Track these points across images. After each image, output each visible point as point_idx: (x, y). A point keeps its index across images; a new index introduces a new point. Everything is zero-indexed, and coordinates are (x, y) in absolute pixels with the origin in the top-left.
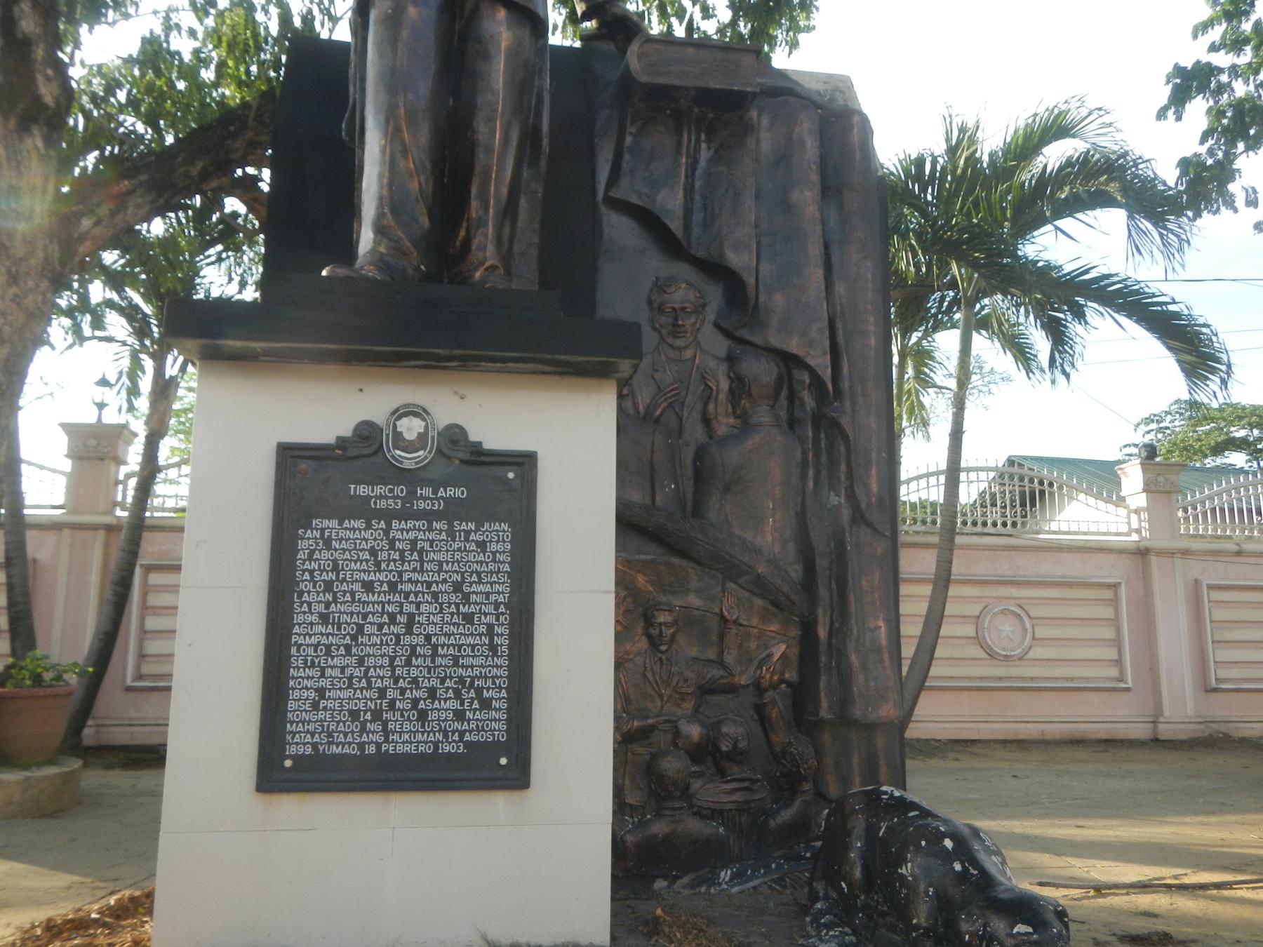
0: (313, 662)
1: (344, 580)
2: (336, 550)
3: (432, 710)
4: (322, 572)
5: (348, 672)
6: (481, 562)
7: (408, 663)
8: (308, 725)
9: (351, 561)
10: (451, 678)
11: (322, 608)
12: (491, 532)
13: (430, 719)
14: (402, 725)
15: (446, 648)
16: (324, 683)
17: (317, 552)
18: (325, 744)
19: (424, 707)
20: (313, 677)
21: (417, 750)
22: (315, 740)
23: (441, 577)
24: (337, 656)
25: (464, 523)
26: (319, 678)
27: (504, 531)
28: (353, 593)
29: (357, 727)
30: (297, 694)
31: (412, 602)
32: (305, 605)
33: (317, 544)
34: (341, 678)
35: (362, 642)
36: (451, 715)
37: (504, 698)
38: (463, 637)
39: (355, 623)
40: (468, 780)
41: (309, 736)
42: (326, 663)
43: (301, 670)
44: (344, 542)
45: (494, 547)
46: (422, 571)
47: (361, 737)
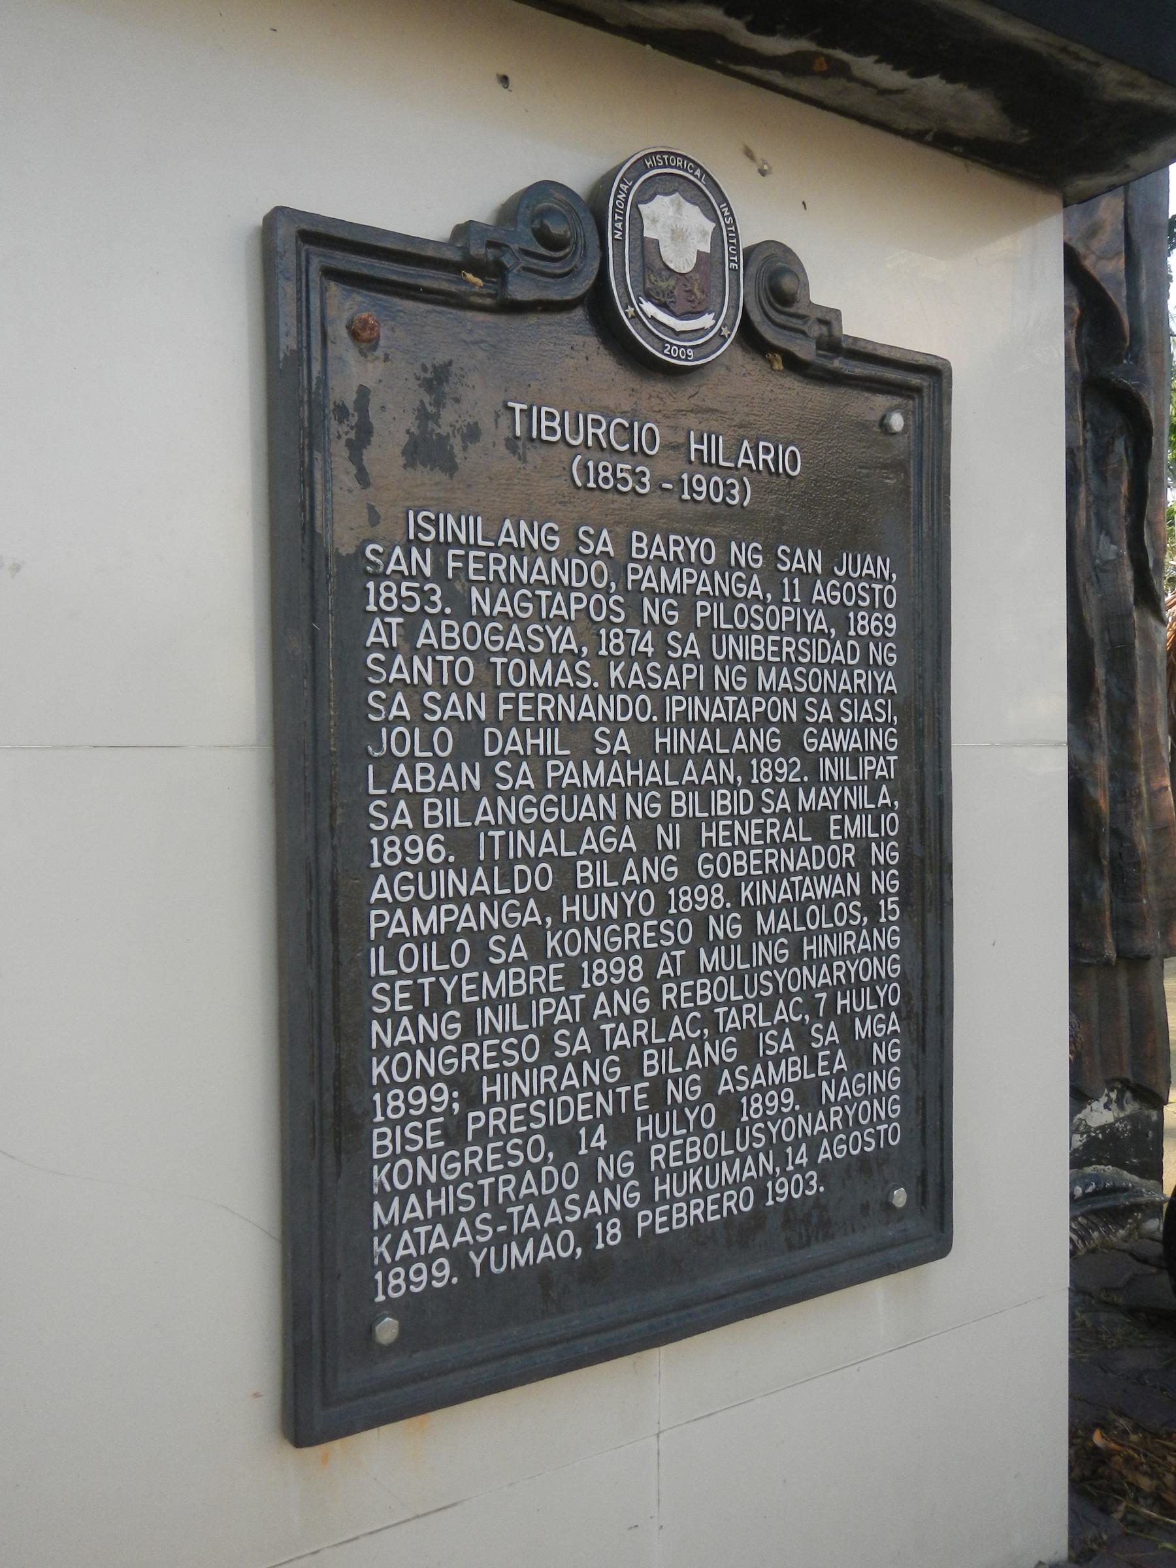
0: (437, 989)
2: (482, 619)
3: (749, 1093)
4: (446, 692)
7: (692, 968)
8: (436, 1196)
9: (527, 656)
10: (788, 996)
13: (745, 1118)
14: (682, 1148)
16: (472, 1055)
17: (427, 624)
18: (488, 1245)
19: (730, 1087)
20: (442, 1041)
22: (458, 1239)
24: (506, 965)
26: (458, 1043)
30: (396, 1102)
33: (426, 596)
34: (520, 1035)
35: (571, 914)
40: (832, 1263)
41: (439, 1229)
43: (405, 1022)
45: (866, 624)
46: (711, 692)
47: (582, 1204)
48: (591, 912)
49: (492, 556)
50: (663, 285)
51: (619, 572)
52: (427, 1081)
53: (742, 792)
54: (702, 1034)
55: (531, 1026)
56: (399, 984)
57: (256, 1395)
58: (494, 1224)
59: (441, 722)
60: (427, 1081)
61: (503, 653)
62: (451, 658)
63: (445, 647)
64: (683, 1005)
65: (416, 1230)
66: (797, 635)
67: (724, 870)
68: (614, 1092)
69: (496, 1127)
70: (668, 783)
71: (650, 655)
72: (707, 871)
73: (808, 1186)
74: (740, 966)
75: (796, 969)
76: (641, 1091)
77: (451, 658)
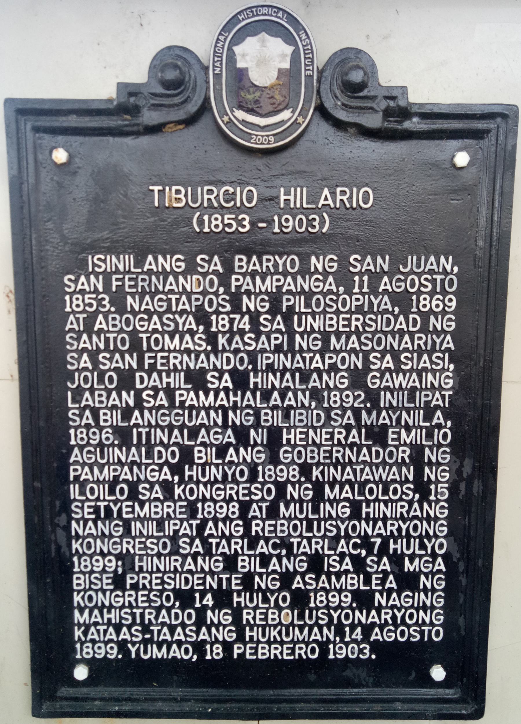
0: (108, 509)
1: (153, 368)
2: (134, 313)
3: (316, 591)
4: (113, 353)
5: (169, 528)
6: (401, 332)
10: (348, 537)
11: (117, 419)
12: (419, 275)
13: (312, 605)
14: (266, 614)
15: (337, 488)
17: (101, 317)
18: (140, 642)
19: (301, 586)
20: (111, 536)
21: (293, 653)
22: (122, 637)
23: (327, 361)
25: (369, 259)
26: (121, 537)
27: (445, 272)
28: (170, 392)
29: (189, 616)
30: (85, 561)
31: (275, 408)
32: (87, 413)
34: (158, 538)
36: (349, 599)
37: (439, 571)
38: (367, 469)
39: (176, 444)
41: (111, 629)
42: (133, 512)
43: (90, 524)
44: (147, 298)
47: (198, 633)
48: (204, 475)
49: (140, 277)
50: (250, 97)
51: (224, 281)
52: (102, 554)
53: (315, 412)
54: (281, 553)
55: (164, 533)
56: (86, 504)
57: (25, 684)
58: (143, 632)
59: (109, 370)
60: (102, 554)
61: (146, 331)
62: (115, 335)
63: (111, 329)
64: (267, 535)
65: (98, 627)
66: (364, 314)
67: (299, 458)
68: (218, 577)
69: (144, 584)
70: (258, 405)
71: (247, 330)
72: (286, 458)
73: (361, 651)
74: (310, 516)
75: (356, 523)
76: (236, 578)
77: (115, 335)
